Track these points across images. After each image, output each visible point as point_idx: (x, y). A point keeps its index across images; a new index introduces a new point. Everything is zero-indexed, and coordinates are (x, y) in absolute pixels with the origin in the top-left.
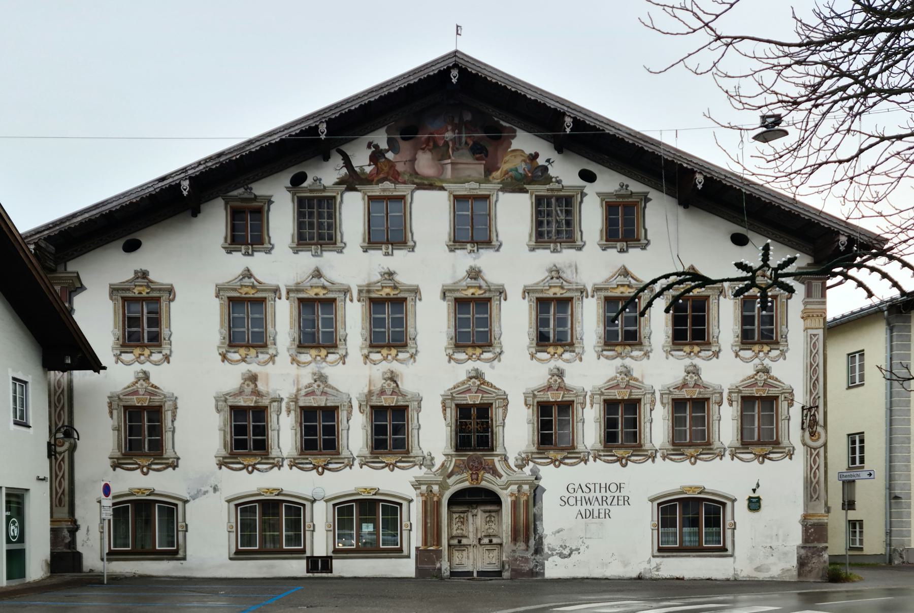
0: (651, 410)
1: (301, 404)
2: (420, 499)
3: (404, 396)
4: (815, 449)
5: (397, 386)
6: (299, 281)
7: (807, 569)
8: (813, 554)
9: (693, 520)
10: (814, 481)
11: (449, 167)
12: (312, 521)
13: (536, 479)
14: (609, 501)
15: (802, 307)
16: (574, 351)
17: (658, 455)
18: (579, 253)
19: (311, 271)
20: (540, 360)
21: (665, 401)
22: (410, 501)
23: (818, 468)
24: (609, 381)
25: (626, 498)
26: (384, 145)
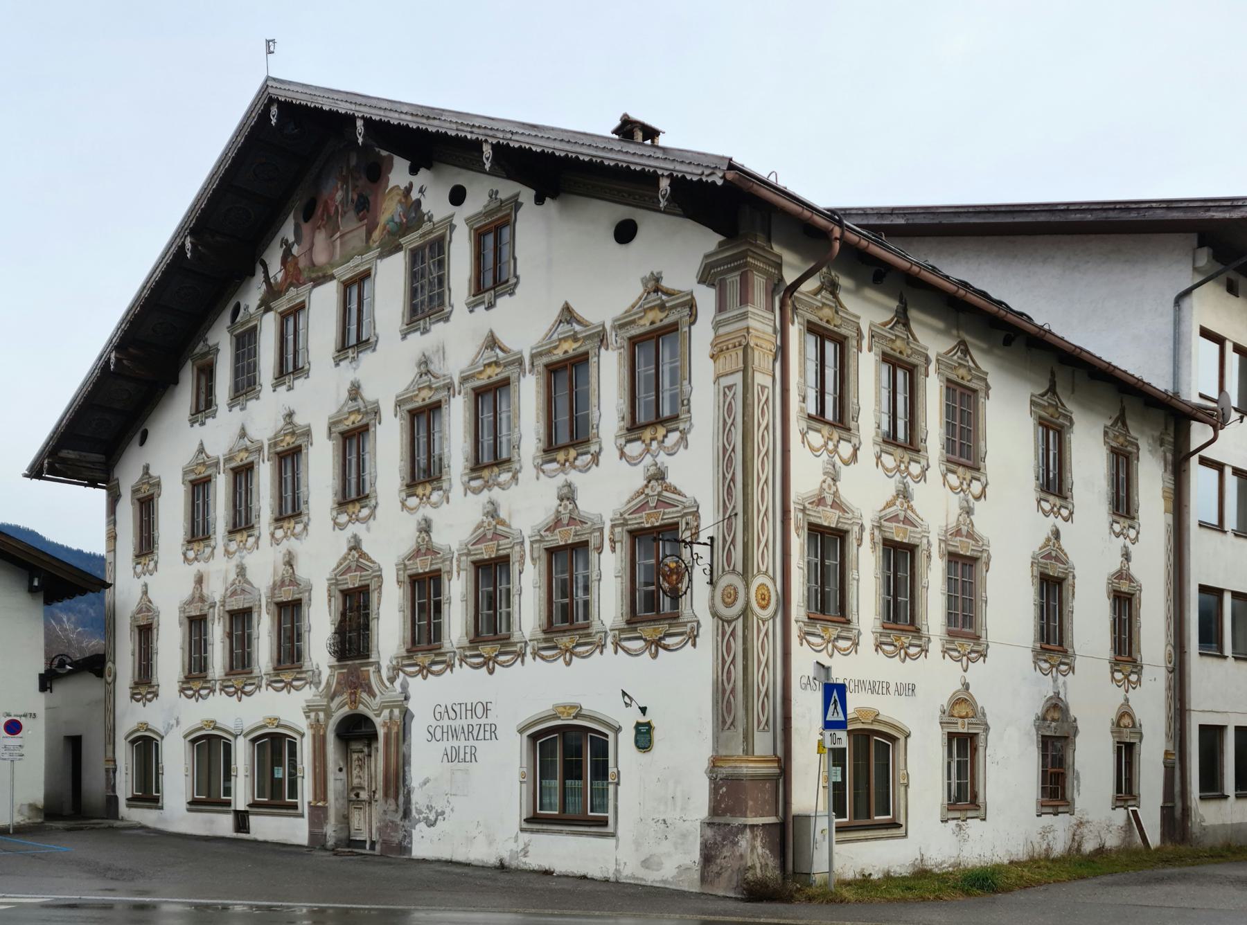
4: (729, 622)
7: (715, 868)
8: (724, 839)
9: (571, 764)
10: (728, 688)
11: (338, 242)
14: (475, 733)
15: (712, 335)
16: (440, 489)
21: (536, 555)
22: (303, 735)
23: (733, 662)
24: (475, 531)
26: (291, 239)
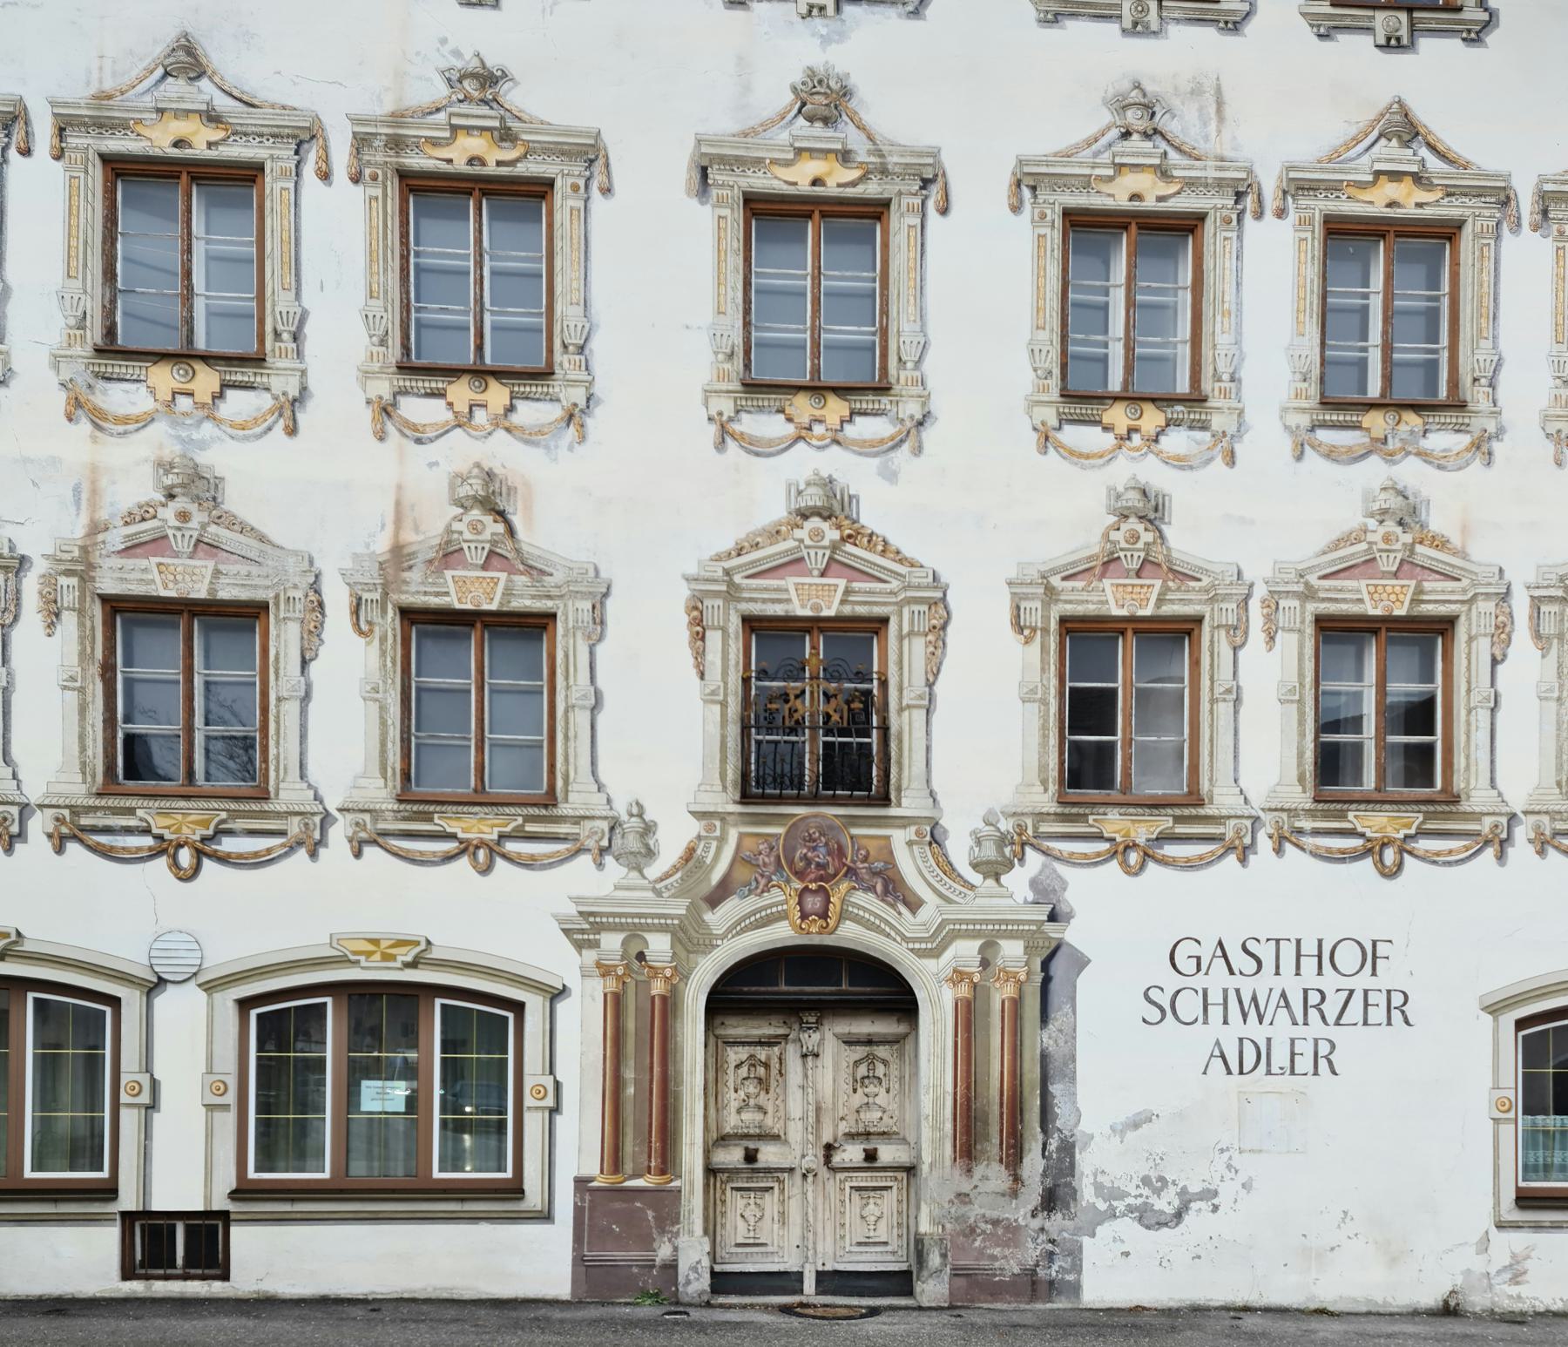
0: (1495, 662)
1: (109, 586)
2: (598, 988)
3: (535, 572)
5: (511, 531)
6: (108, 85)
12: (148, 1069)
13: (1053, 917)
16: (1204, 427)
17: (1521, 833)
18: (1230, 40)
19: (159, 50)
20: (1074, 455)
21: (1548, 628)
22: (557, 994)
24: (1337, 545)
25: (1397, 1000)
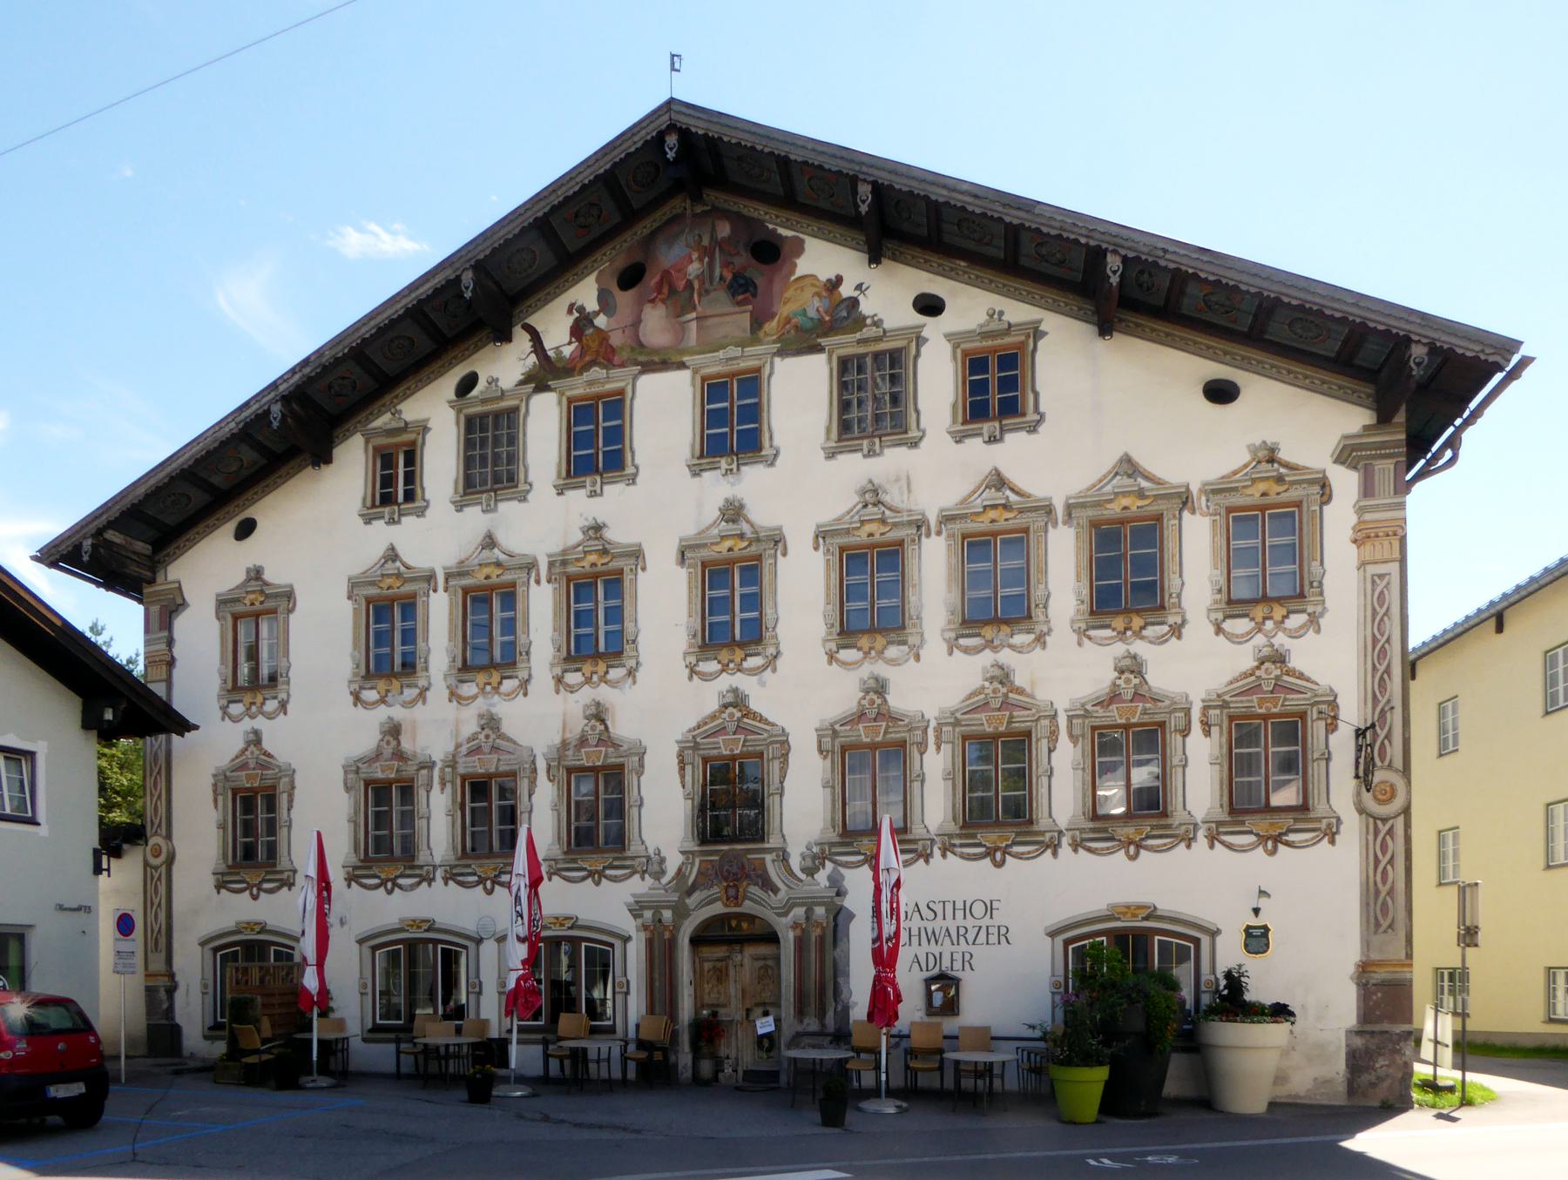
0: (1050, 751)
1: (461, 770)
2: (643, 935)
3: (616, 746)
4: (1384, 820)
5: (607, 728)
6: (463, 557)
10: (1384, 890)
11: (694, 325)
12: (478, 976)
13: (838, 894)
14: (971, 937)
15: (1354, 519)
16: (904, 643)
17: (1065, 841)
18: (914, 451)
19: (480, 538)
20: (844, 664)
21: (1077, 731)
22: (626, 940)
24: (969, 697)
25: (1003, 931)
26: (592, 305)
